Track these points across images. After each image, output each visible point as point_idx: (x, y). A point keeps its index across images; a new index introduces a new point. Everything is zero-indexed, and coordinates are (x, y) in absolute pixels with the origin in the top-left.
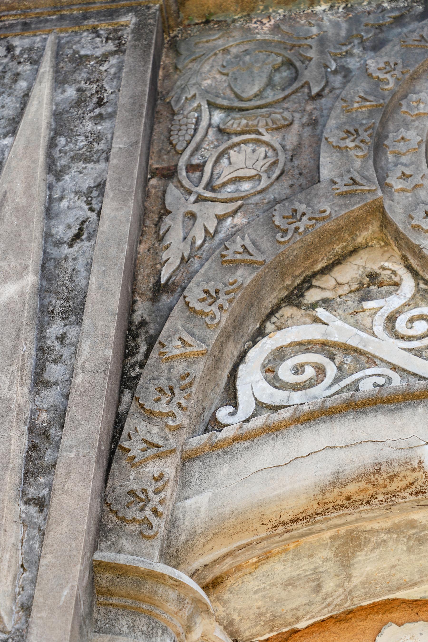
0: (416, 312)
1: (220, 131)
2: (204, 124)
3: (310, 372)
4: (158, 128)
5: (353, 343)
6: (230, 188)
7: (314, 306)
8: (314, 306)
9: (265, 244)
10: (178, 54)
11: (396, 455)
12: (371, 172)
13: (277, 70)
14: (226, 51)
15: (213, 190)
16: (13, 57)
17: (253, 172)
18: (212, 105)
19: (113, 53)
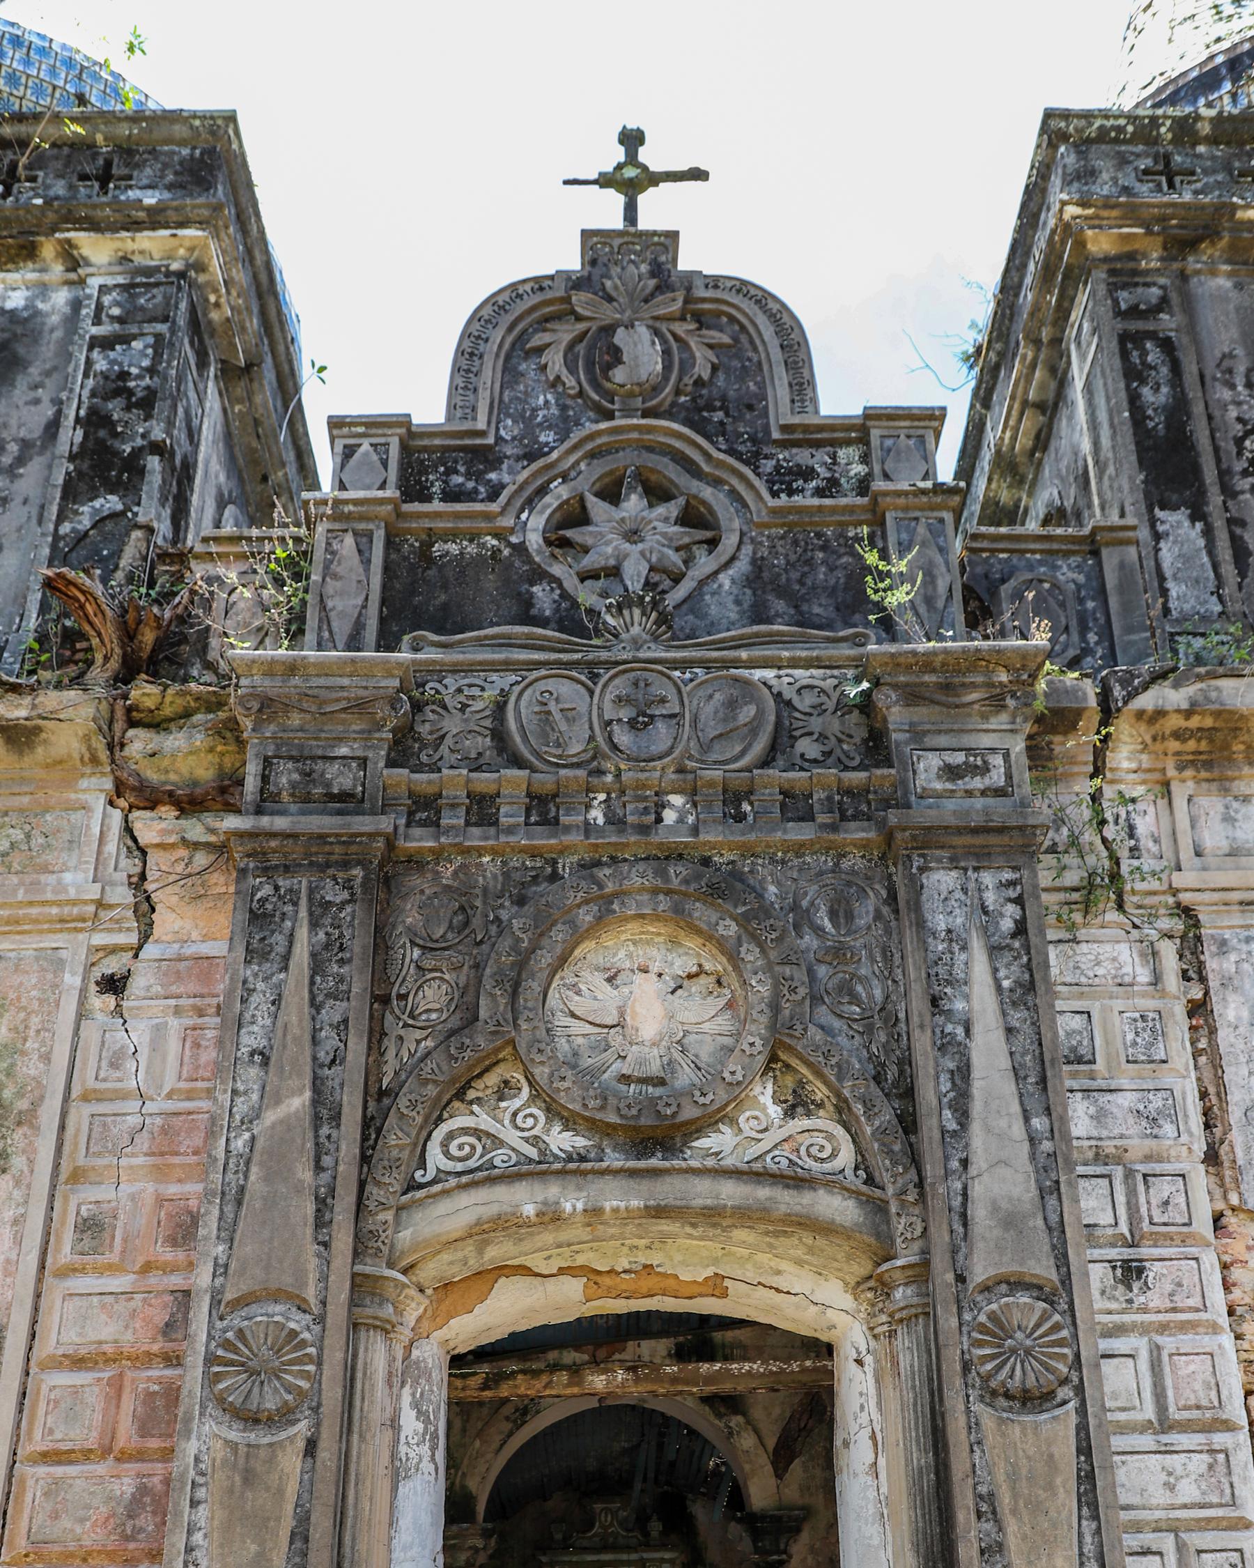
0: (528, 1111)
1: (418, 967)
2: (407, 960)
3: (467, 1149)
4: (378, 959)
5: (492, 1131)
6: (424, 1017)
7: (471, 1102)
8: (471, 1102)
9: (445, 1068)
10: (389, 891)
11: (509, 1209)
12: (509, 1016)
13: (455, 913)
14: (422, 892)
15: (413, 1018)
16: (280, 897)
17: (438, 1006)
18: (413, 943)
19: (349, 902)
